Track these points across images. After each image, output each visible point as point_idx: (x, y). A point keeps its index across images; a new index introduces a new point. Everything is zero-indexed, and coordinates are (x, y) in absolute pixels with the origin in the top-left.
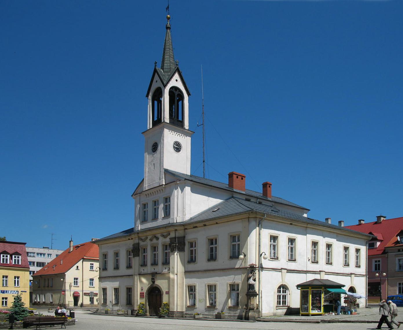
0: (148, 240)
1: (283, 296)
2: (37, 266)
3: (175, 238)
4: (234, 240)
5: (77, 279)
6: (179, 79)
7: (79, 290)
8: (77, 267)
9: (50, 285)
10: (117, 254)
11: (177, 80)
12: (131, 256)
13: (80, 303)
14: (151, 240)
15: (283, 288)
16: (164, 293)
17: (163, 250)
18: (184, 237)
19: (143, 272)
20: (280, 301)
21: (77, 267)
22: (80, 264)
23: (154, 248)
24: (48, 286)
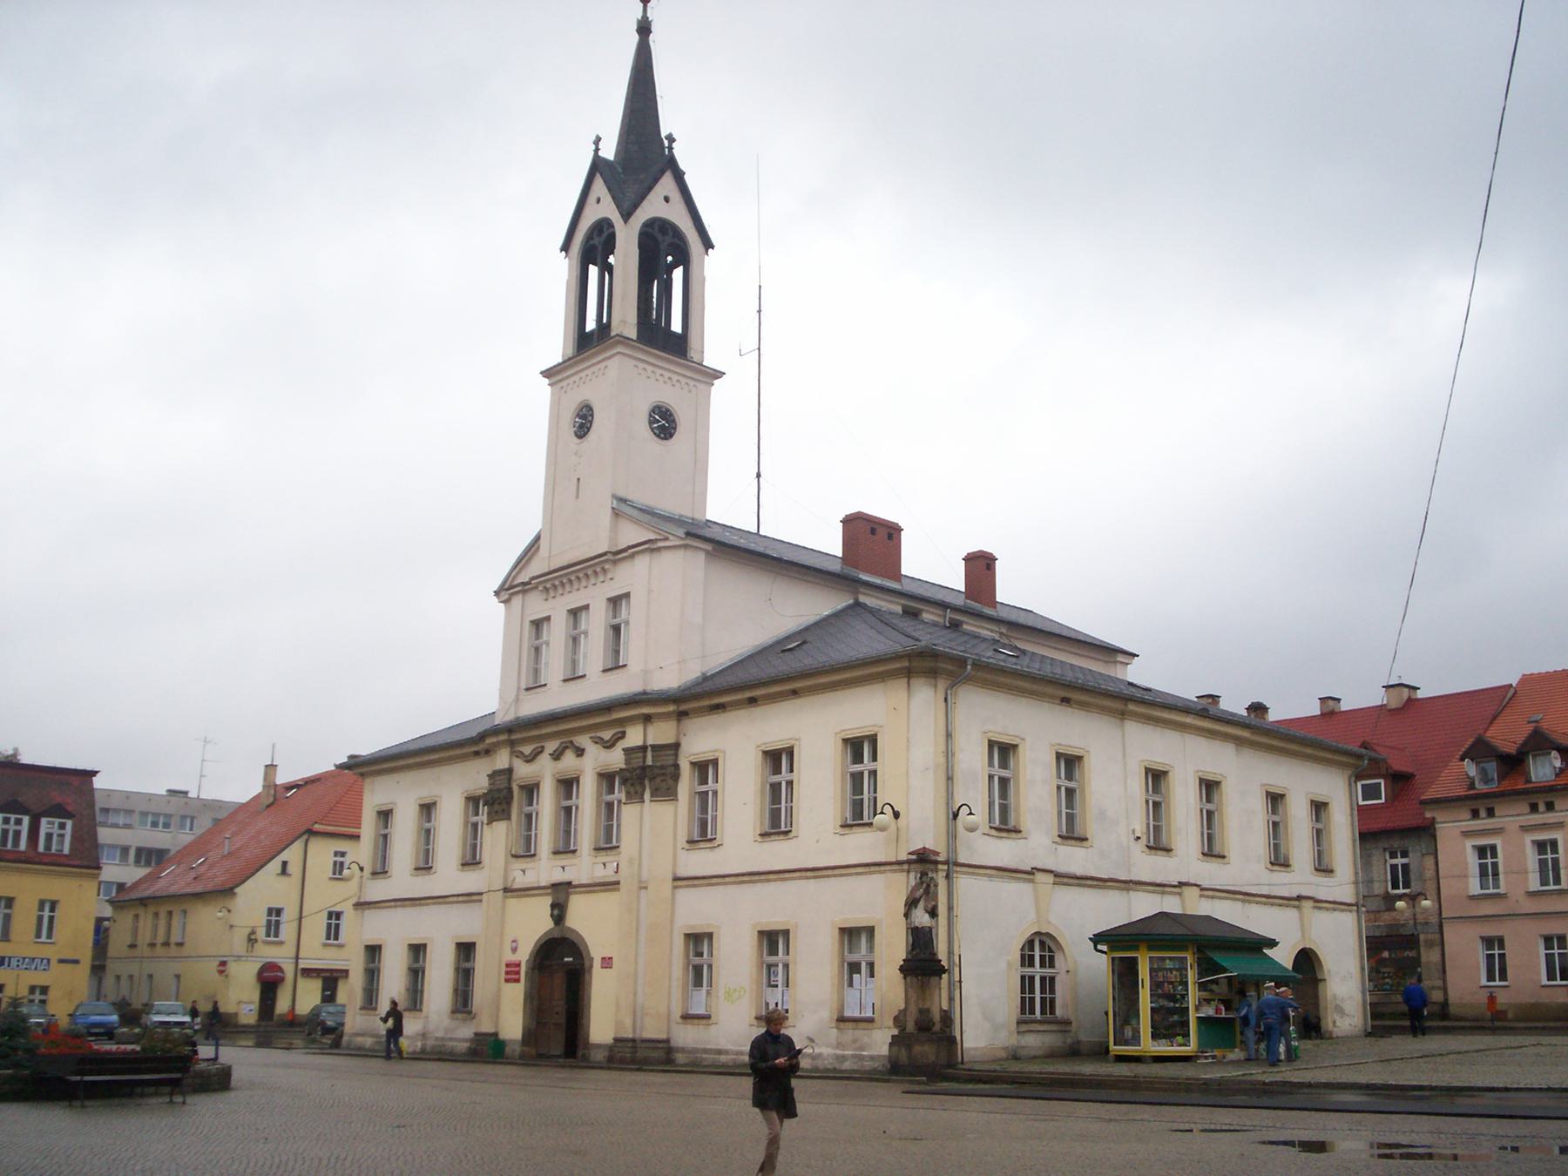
0: (545, 760)
1: (1043, 979)
2: (137, 862)
3: (643, 748)
4: (858, 758)
5: (279, 912)
6: (676, 196)
7: (281, 955)
8: (285, 864)
9: (175, 938)
10: (427, 809)
11: (667, 199)
12: (483, 817)
13: (282, 1006)
14: (557, 756)
15: (1040, 949)
17: (599, 794)
18: (676, 746)
19: (520, 881)
20: (1032, 1000)
21: (285, 864)
22: (292, 854)
23: (568, 785)
24: (166, 944)
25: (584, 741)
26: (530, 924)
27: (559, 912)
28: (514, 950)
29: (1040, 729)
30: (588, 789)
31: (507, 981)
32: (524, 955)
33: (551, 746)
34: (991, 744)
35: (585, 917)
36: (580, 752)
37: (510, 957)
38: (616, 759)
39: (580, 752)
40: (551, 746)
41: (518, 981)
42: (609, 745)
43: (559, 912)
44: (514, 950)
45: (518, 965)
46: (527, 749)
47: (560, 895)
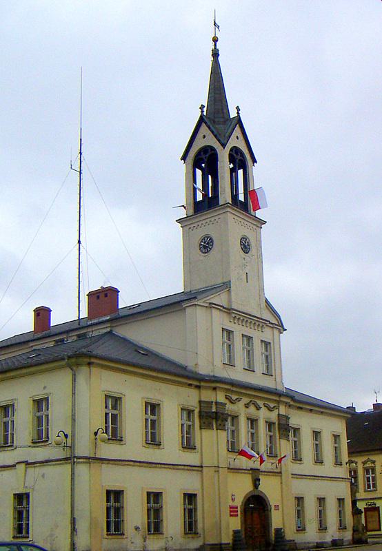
0: (241, 405)
14: (247, 406)
16: (273, 507)
25: (260, 403)
26: (240, 488)
27: (256, 482)
28: (233, 500)
29: (135, 393)
30: (262, 426)
31: (231, 516)
32: (239, 502)
33: (245, 400)
34: (146, 403)
35: (269, 488)
36: (258, 408)
37: (231, 503)
38: (273, 416)
39: (258, 408)
40: (245, 400)
41: (237, 515)
42: (270, 410)
43: (256, 482)
44: (233, 500)
45: (237, 508)
46: (234, 397)
47: (256, 475)
